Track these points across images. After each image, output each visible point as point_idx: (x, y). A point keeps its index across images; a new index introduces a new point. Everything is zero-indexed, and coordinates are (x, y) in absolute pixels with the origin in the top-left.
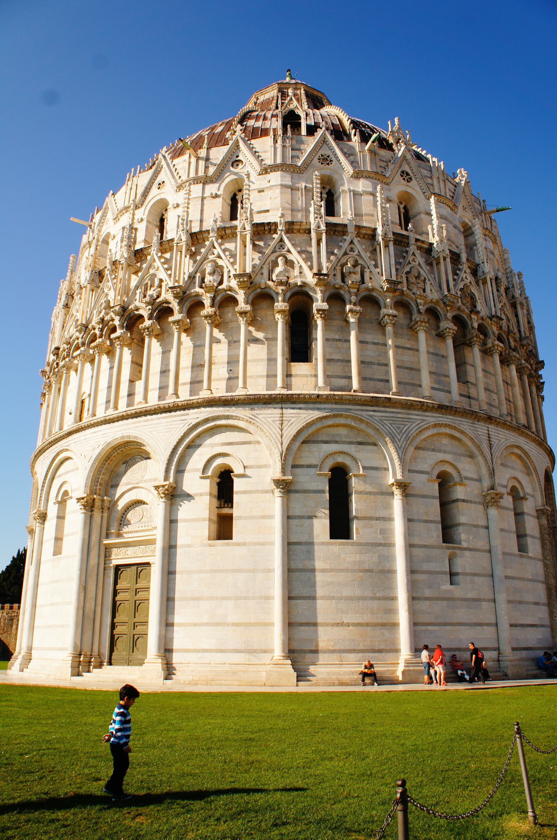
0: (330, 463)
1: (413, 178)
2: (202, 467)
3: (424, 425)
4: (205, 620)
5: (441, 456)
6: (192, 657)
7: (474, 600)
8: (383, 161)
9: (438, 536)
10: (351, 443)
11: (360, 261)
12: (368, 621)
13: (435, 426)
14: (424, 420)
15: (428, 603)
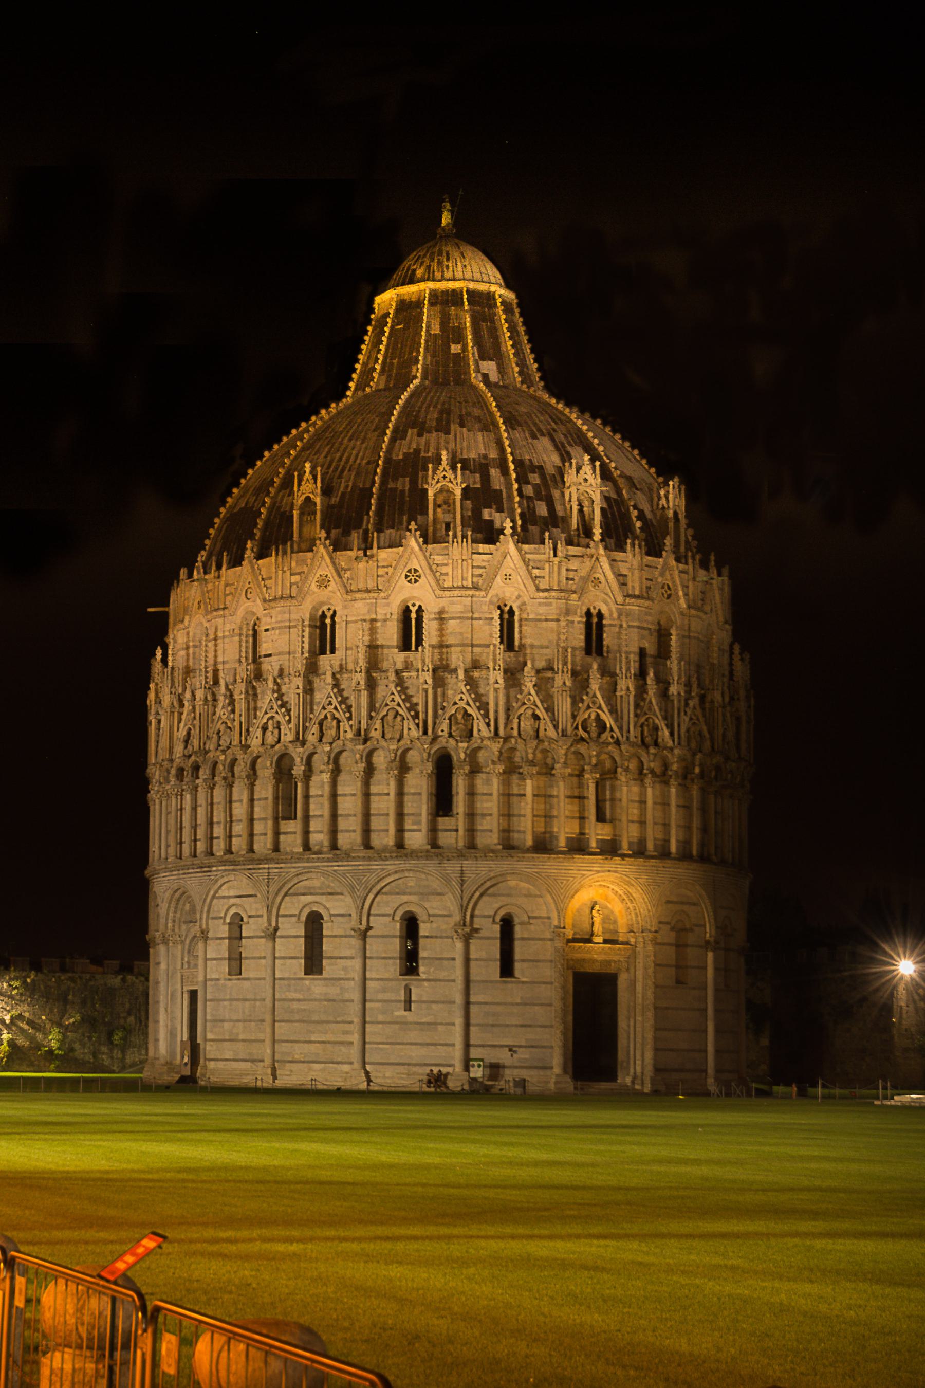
0: (306, 911)
1: (422, 575)
2: (222, 915)
3: (383, 874)
4: (227, 1038)
5: (405, 898)
6: (221, 1065)
7: (429, 1024)
8: (384, 567)
9: (395, 970)
10: (323, 894)
11: (337, 715)
12: (328, 1039)
13: (396, 872)
14: (383, 869)
15: (381, 1026)
